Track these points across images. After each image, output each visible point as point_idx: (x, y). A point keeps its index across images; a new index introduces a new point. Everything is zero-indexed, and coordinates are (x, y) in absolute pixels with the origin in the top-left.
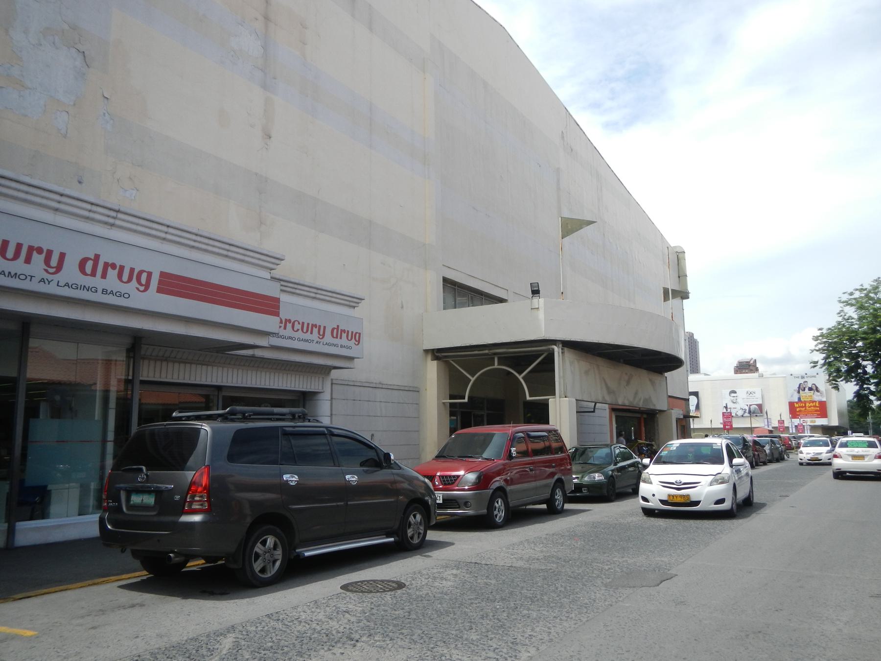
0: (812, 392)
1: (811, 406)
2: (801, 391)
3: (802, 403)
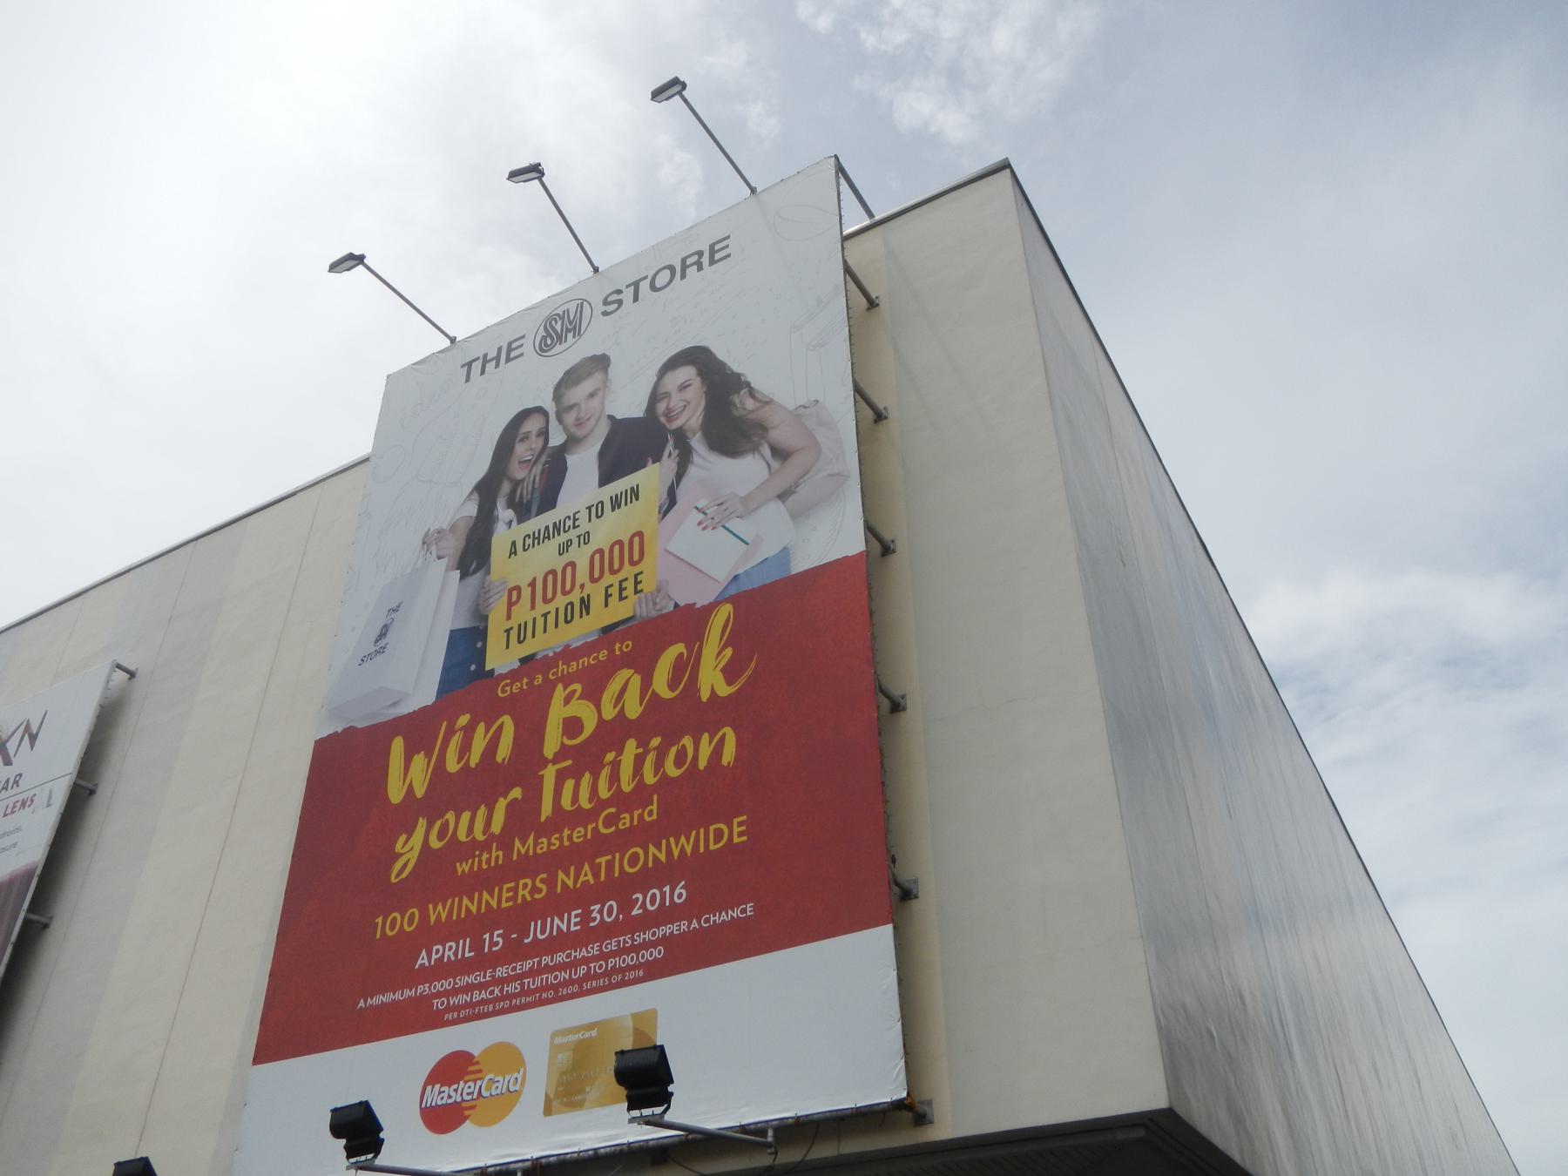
0: (651, 478)
1: (613, 733)
3: (488, 712)
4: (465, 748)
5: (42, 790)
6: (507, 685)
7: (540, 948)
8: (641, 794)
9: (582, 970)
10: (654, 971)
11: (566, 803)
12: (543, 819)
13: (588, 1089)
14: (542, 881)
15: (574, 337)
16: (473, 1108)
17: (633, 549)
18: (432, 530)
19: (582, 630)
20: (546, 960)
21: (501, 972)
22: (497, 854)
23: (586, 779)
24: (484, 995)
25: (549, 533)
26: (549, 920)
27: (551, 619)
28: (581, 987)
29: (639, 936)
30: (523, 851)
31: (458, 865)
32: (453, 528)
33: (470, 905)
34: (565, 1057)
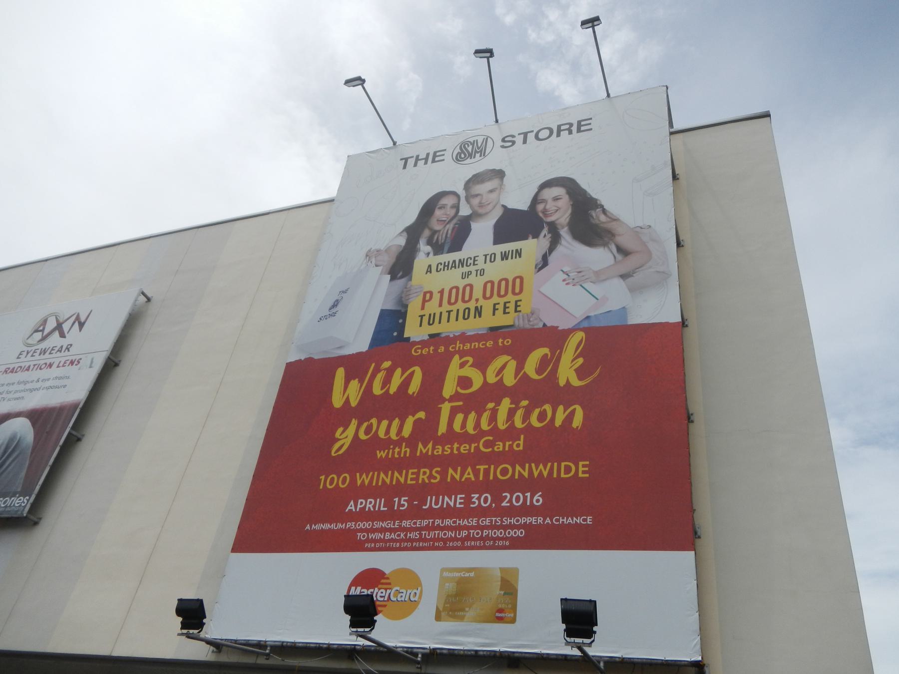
0: (532, 247)
1: (495, 392)
2: (424, 258)
3: (405, 362)
4: (387, 381)
5: (86, 357)
6: (418, 348)
7: (431, 513)
8: (511, 433)
9: (464, 533)
10: (516, 544)
11: (457, 427)
12: (440, 433)
13: (467, 609)
14: (437, 472)
15: (481, 156)
16: (385, 606)
17: (516, 285)
18: (373, 249)
19: (474, 326)
20: (438, 522)
21: (406, 524)
22: (405, 450)
23: (472, 416)
24: (393, 536)
25: (455, 265)
26: (441, 497)
27: (453, 315)
28: (463, 543)
29: (507, 520)
30: (424, 451)
31: (378, 452)
32: (387, 250)
33: (385, 478)
34: (451, 587)
